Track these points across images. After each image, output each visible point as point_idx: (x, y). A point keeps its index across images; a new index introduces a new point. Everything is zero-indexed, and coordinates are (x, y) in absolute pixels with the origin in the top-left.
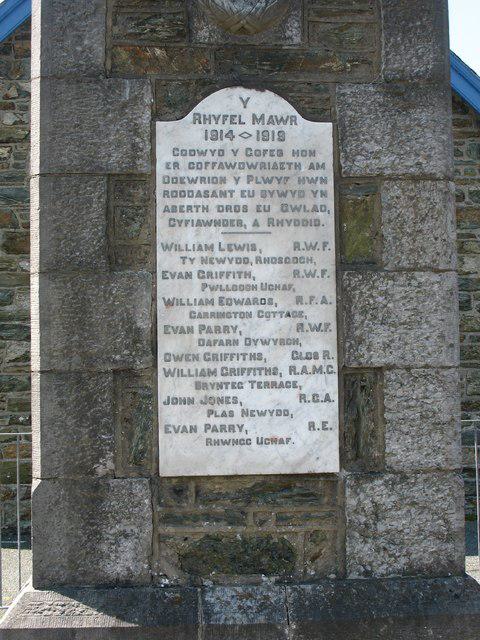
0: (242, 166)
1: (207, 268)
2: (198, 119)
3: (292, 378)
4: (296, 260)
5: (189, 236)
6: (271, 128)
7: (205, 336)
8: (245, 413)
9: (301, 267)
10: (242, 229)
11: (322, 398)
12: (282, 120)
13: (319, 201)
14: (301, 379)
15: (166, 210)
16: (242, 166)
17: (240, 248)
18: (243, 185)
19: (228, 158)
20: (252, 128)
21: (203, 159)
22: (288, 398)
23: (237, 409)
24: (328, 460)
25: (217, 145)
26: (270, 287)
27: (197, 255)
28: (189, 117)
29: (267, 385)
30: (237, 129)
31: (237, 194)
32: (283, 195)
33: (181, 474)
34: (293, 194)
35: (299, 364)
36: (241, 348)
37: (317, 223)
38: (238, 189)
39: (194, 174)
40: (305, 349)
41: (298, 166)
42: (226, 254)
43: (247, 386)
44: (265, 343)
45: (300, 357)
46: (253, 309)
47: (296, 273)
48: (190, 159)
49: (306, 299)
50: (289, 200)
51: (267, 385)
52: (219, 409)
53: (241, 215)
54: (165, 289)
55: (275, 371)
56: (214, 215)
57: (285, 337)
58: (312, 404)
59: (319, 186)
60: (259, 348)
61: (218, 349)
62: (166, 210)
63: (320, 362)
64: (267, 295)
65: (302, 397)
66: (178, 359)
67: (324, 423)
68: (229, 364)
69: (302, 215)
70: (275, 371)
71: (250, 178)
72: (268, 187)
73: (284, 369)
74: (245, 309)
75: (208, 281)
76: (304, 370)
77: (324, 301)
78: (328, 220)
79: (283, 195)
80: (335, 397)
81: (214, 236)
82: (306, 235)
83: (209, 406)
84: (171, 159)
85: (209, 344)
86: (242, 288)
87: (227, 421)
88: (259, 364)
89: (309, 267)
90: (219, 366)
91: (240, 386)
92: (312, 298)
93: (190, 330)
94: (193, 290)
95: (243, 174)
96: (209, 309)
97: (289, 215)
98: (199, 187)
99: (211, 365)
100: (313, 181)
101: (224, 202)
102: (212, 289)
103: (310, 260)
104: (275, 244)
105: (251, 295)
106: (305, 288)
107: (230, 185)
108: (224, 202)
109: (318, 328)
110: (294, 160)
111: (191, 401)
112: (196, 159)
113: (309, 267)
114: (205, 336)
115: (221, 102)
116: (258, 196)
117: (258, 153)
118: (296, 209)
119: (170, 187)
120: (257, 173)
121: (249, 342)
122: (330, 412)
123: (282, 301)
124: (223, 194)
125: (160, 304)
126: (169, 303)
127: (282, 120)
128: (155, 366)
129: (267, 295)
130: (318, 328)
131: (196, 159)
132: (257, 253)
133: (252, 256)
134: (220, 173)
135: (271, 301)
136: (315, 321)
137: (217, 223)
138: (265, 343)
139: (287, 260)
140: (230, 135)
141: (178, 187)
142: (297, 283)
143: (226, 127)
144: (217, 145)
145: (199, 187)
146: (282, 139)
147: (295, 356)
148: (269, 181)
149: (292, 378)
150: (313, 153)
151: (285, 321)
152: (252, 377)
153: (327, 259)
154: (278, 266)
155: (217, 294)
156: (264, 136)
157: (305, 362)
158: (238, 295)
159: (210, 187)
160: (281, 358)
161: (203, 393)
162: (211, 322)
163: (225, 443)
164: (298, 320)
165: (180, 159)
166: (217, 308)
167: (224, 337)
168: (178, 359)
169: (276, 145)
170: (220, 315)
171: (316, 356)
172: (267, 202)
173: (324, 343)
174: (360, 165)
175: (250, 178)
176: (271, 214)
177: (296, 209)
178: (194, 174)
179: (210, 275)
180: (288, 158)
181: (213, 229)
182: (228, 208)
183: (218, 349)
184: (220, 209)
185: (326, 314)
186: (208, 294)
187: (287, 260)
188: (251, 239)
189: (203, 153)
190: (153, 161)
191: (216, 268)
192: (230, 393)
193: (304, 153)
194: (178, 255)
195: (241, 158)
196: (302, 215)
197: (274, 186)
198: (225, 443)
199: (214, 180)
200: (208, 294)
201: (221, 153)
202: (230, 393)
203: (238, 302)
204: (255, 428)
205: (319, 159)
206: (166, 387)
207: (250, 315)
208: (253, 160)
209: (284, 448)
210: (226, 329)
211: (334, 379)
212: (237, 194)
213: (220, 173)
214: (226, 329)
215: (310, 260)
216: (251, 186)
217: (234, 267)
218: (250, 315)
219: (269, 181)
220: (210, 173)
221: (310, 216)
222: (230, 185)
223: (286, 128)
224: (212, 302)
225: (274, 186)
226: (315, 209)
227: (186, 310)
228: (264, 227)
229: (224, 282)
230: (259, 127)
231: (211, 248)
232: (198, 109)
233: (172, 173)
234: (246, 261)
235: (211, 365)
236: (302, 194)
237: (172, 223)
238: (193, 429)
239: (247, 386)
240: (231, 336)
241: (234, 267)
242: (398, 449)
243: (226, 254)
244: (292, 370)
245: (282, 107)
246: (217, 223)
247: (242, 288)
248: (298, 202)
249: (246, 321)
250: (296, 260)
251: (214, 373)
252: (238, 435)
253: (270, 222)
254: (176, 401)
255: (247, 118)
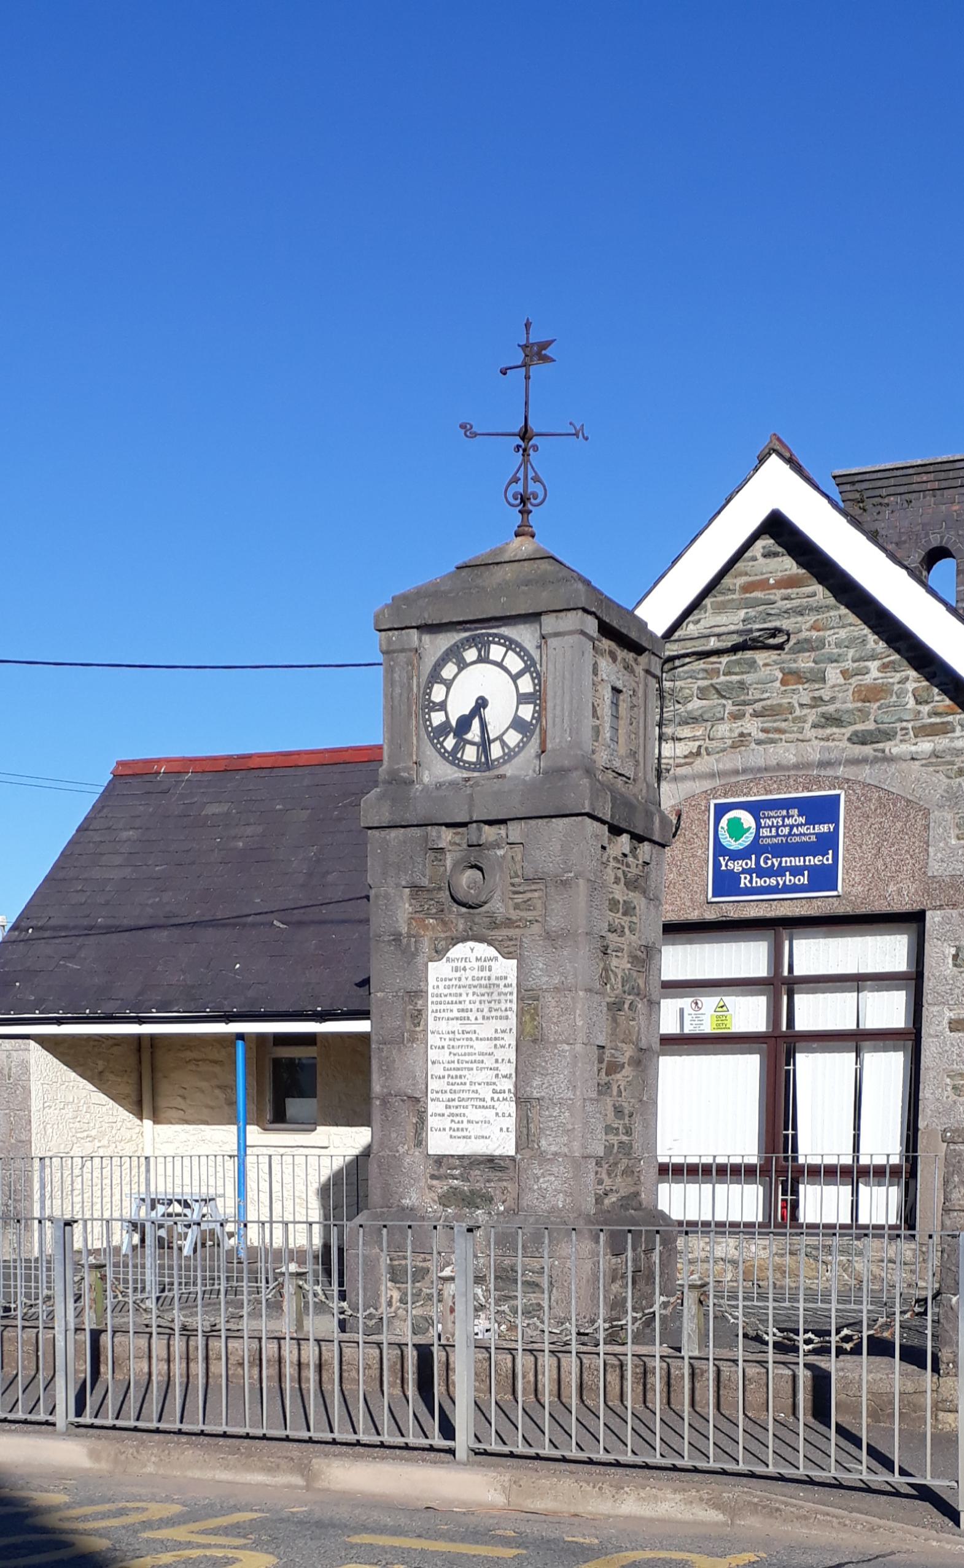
0: (470, 986)
1: (452, 1043)
2: (448, 960)
3: (492, 1103)
4: (496, 1039)
5: (443, 1026)
6: (485, 964)
7: (451, 1080)
8: (469, 1122)
9: (498, 1043)
10: (469, 1022)
11: (507, 1115)
12: (491, 959)
13: (508, 1005)
14: (496, 1104)
15: (433, 1011)
16: (470, 986)
17: (468, 1033)
18: (471, 997)
19: (463, 982)
20: (476, 965)
21: (451, 983)
22: (490, 1114)
23: (465, 1119)
24: (508, 1148)
25: (458, 975)
26: (482, 1054)
27: (447, 1036)
28: (445, 959)
29: (480, 1107)
30: (468, 965)
31: (467, 1002)
32: (490, 1002)
33: (439, 1153)
34: (495, 1001)
35: (496, 1096)
36: (467, 1087)
37: (507, 1018)
38: (467, 1000)
39: (447, 991)
40: (498, 1088)
41: (498, 986)
42: (461, 1036)
43: (470, 1107)
44: (479, 1084)
45: (497, 1092)
46: (474, 1066)
47: (495, 1046)
48: (444, 983)
49: (500, 1061)
50: (492, 1005)
51: (480, 1107)
52: (456, 1119)
53: (469, 1014)
54: (432, 1054)
55: (484, 1100)
56: (456, 1014)
57: (489, 1081)
58: (502, 1118)
59: (509, 997)
60: (477, 1087)
61: (456, 1087)
62: (433, 1011)
63: (506, 1095)
64: (481, 1058)
65: (497, 1114)
66: (437, 1092)
67: (508, 1129)
68: (462, 1095)
69: (499, 1014)
70: (484, 1100)
71: (474, 994)
72: (483, 998)
73: (488, 1099)
74: (470, 1065)
75: (453, 1051)
76: (498, 1100)
77: (509, 1061)
78: (513, 1016)
79: (490, 1002)
80: (514, 1115)
81: (456, 1026)
82: (501, 1025)
83: (451, 1118)
84: (436, 984)
85: (452, 1084)
86: (469, 1054)
87: (460, 1126)
88: (476, 1096)
89: (502, 1042)
90: (456, 1096)
91: (467, 1107)
92: (503, 1060)
93: (444, 1077)
94: (444, 1055)
95: (470, 992)
96: (452, 1066)
97: (494, 1014)
98: (449, 999)
99: (453, 1096)
100: (506, 994)
101: (460, 1006)
102: (455, 1055)
103: (503, 1039)
104: (487, 1029)
105: (473, 1058)
106: (499, 1054)
107: (464, 997)
108: (460, 1006)
109: (505, 1077)
110: (497, 982)
111: (443, 1115)
112: (448, 983)
113: (502, 1042)
114: (451, 1080)
115: (459, 950)
116: (478, 1003)
117: (478, 979)
118: (496, 1010)
119: (435, 999)
120: (478, 990)
121: (471, 1083)
122: (511, 1123)
123: (489, 1062)
124: (460, 1002)
125: (429, 1063)
126: (433, 1063)
127: (491, 959)
128: (427, 1096)
129: (481, 1058)
130: (505, 1077)
131: (448, 983)
132: (476, 1035)
133: (474, 1036)
134: (458, 991)
135: (482, 1062)
136: (504, 1073)
137: (457, 1019)
138: (479, 1084)
139: (491, 1039)
140: (465, 969)
141: (439, 999)
142: (495, 1052)
143: (462, 965)
144: (458, 975)
145: (449, 999)
146: (490, 970)
147: (495, 1092)
148: (483, 995)
149: (492, 1103)
150: (506, 978)
151: (490, 1072)
152: (472, 1103)
153: (511, 1039)
154: (487, 1042)
155: (457, 1058)
156: (482, 969)
157: (499, 1095)
158: (467, 1058)
159: (454, 999)
160: (486, 1092)
161: (449, 1111)
162: (453, 1073)
163: (459, 1138)
164: (496, 1072)
165: (440, 983)
166: (456, 1065)
167: (459, 1081)
168: (437, 1092)
169: (486, 974)
170: (458, 1069)
171: (504, 1092)
172: (482, 1006)
173: (508, 1085)
174: (531, 984)
175: (474, 994)
176: (484, 1013)
177: (496, 1010)
178: (447, 991)
179: (453, 1047)
180: (493, 981)
181: (455, 1021)
182: (463, 1010)
183: (456, 1087)
184: (459, 1011)
185: (510, 1069)
186: (452, 1058)
187: (491, 1039)
188: (473, 1028)
189: (450, 980)
190: (427, 985)
191: (457, 1043)
192: (462, 1111)
193: (501, 978)
194: (438, 1036)
195: (470, 982)
196: (499, 1014)
197: (486, 998)
198: (459, 1138)
199: (456, 995)
200: (452, 1058)
201: (460, 979)
202: (462, 1111)
203: (467, 1062)
204: (474, 1130)
205: (509, 981)
206: (432, 1108)
207: (472, 1069)
208: (476, 983)
209: (487, 1141)
210: (461, 1077)
211: (513, 1104)
212: (467, 1002)
213: (458, 991)
214: (461, 1077)
215: (503, 1039)
216: (475, 998)
217: (465, 1043)
218: (472, 1069)
219: (483, 995)
220: (453, 991)
221: (504, 1014)
222: (464, 997)
223: (492, 963)
224: (453, 1062)
225: (486, 998)
226: (506, 1010)
227: (442, 1066)
228: (480, 1021)
229: (460, 1051)
230: (480, 964)
231: (453, 1032)
232: (449, 955)
233: (436, 991)
234: (471, 1039)
235: (453, 1096)
236: (499, 1002)
237: (435, 1019)
238: (444, 1129)
239: (470, 1107)
240: (463, 1080)
241: (465, 1043)
242: (548, 1144)
243: (461, 1036)
244: (492, 1099)
245: (491, 952)
246: (457, 1019)
247: (469, 1054)
248: (497, 1006)
249: (470, 1072)
250: (496, 1039)
251: (453, 1100)
252: (465, 1133)
253: (483, 1018)
254: (436, 1115)
255: (473, 959)
